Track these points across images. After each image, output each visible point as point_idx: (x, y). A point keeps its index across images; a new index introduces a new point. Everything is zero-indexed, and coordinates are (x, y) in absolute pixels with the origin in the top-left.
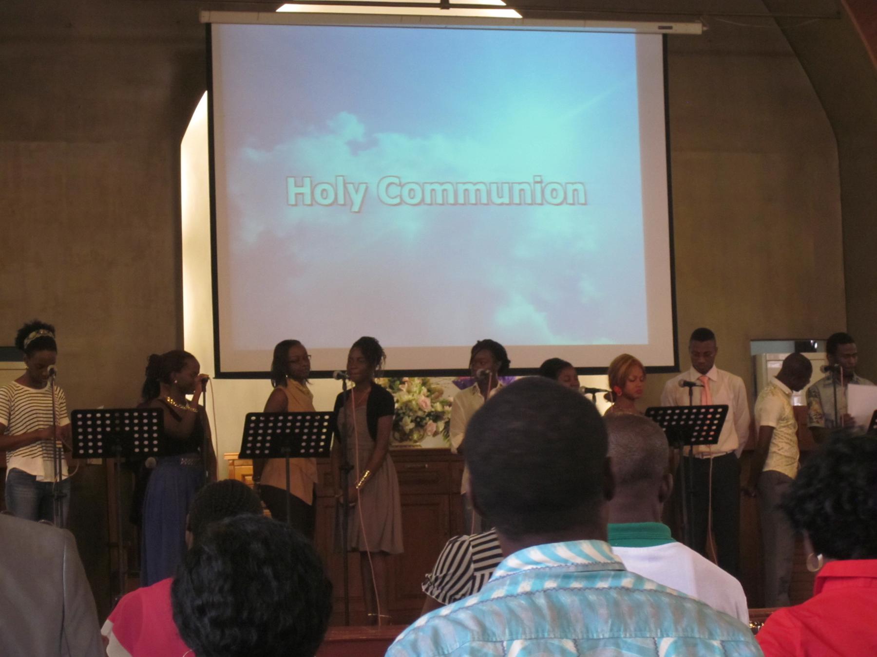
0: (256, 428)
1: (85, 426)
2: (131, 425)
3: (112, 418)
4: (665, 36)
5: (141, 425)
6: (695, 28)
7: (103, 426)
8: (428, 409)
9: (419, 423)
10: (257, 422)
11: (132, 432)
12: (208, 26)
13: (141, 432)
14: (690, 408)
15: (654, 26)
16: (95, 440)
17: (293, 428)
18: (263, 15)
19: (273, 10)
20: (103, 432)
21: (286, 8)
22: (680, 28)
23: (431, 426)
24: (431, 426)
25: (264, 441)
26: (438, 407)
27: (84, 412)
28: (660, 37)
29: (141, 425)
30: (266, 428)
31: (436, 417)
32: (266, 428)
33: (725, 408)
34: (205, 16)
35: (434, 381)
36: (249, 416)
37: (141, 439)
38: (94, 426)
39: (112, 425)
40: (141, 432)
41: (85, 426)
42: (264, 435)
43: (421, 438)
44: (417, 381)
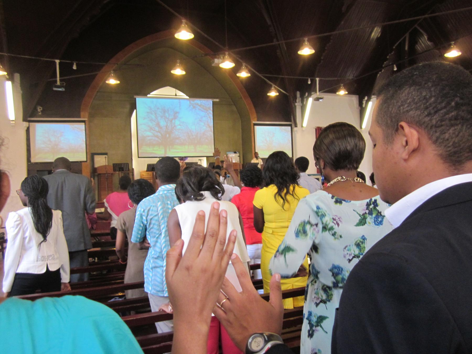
6: (217, 100)
12: (135, 99)
21: (149, 96)
22: (215, 100)
34: (135, 97)
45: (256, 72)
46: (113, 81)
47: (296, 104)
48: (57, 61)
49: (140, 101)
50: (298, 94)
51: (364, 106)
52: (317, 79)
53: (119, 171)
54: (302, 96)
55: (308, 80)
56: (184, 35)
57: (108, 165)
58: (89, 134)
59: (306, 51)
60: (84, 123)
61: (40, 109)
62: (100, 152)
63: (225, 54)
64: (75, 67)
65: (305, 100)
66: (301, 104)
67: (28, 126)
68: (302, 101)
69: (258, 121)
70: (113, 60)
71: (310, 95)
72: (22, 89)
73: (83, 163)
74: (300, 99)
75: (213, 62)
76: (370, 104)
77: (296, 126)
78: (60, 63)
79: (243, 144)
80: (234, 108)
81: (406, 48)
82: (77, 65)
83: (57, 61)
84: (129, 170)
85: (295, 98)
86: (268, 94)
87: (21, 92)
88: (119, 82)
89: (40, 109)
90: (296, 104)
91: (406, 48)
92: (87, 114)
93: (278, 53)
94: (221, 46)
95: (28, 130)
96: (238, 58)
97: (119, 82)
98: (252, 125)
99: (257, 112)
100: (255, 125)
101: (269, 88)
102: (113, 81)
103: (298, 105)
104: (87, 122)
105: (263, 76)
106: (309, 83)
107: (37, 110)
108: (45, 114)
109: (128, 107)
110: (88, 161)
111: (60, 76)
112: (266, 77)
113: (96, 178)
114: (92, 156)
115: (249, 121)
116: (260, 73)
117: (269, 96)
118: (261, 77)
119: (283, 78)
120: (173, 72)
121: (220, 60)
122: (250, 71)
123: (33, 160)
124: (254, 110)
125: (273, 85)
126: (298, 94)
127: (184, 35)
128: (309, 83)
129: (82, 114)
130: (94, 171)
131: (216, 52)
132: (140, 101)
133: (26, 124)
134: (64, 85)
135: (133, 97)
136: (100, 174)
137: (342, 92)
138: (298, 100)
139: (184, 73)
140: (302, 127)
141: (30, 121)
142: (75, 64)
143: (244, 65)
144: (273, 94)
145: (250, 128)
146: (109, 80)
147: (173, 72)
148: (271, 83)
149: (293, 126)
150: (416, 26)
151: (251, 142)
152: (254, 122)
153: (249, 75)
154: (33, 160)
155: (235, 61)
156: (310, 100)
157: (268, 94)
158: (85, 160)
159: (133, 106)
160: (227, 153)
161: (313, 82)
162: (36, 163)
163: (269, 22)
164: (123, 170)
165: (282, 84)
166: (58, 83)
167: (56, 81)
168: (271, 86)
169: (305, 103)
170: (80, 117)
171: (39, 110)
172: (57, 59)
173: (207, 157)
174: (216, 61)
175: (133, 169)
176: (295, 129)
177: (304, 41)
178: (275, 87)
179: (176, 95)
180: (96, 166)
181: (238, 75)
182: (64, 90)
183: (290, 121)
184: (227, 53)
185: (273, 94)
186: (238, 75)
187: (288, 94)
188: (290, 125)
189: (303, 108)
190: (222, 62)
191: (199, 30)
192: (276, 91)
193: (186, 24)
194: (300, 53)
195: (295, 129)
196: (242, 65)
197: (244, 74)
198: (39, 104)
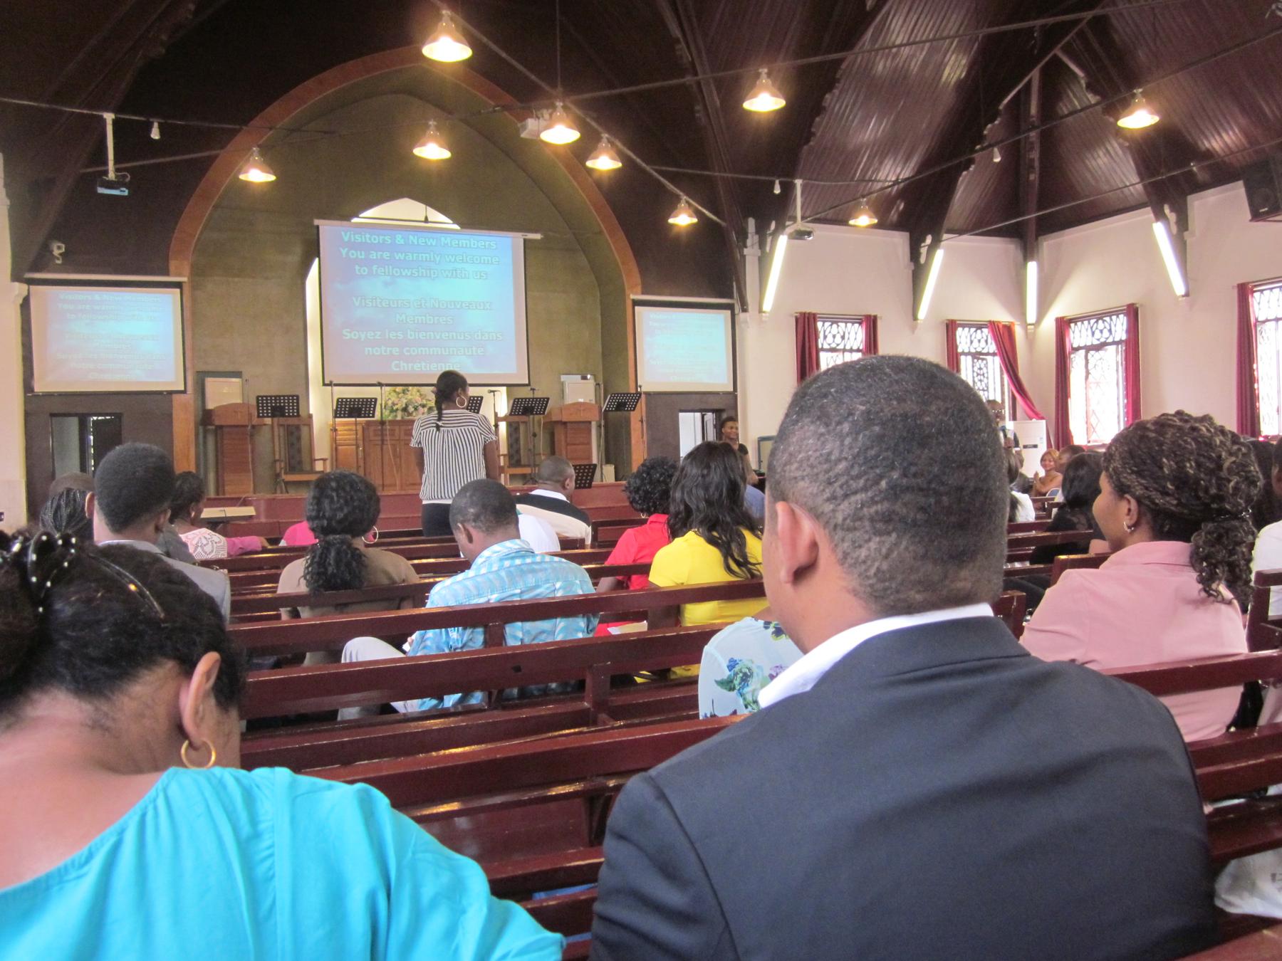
6: (538, 236)
9: (416, 409)
21: (355, 220)
22: (531, 236)
31: (424, 406)
34: (316, 222)
44: (416, 388)
45: (638, 160)
46: (257, 176)
47: (746, 251)
48: (109, 117)
49: (328, 230)
50: (751, 223)
51: (922, 260)
52: (798, 183)
53: (273, 416)
54: (761, 230)
55: (773, 184)
56: (447, 49)
58: (192, 321)
61: (58, 249)
62: (221, 369)
64: (155, 134)
65: (769, 239)
67: (25, 293)
68: (762, 244)
70: (257, 122)
71: (781, 228)
72: (8, 195)
73: (175, 397)
74: (756, 238)
75: (524, 128)
76: (939, 255)
77: (744, 310)
79: (604, 355)
80: (583, 260)
81: (1034, 110)
82: (161, 127)
83: (109, 117)
84: (298, 415)
85: (743, 235)
86: (671, 221)
87: (8, 202)
88: (272, 178)
89: (58, 249)
91: (1034, 110)
92: (187, 269)
94: (547, 88)
95: (25, 305)
97: (272, 178)
98: (629, 304)
99: (643, 271)
100: (636, 303)
101: (671, 205)
102: (257, 176)
103: (751, 252)
104: (186, 288)
105: (656, 171)
106: (777, 191)
108: (70, 261)
109: (298, 250)
110: (190, 390)
111: (116, 161)
115: (622, 293)
117: (672, 225)
118: (651, 176)
120: (418, 151)
121: (542, 123)
122: (621, 156)
123: (39, 387)
125: (684, 198)
126: (751, 223)
127: (447, 49)
128: (777, 191)
129: (173, 264)
130: (206, 418)
132: (328, 230)
133: (20, 289)
134: (128, 179)
136: (221, 427)
137: (864, 220)
138: (752, 239)
139: (445, 154)
140: (760, 311)
141: (31, 282)
142: (156, 125)
144: (683, 220)
145: (625, 311)
146: (246, 172)
147: (418, 151)
148: (678, 192)
149: (737, 308)
150: (1057, 51)
152: (632, 297)
153: (620, 165)
154: (39, 387)
156: (783, 241)
157: (671, 221)
159: (312, 249)
161: (788, 188)
163: (677, 33)
164: (283, 415)
165: (706, 194)
166: (112, 175)
167: (106, 173)
168: (678, 199)
169: (768, 249)
170: (167, 273)
171: (56, 252)
172: (107, 110)
174: (531, 123)
175: (310, 416)
176: (741, 317)
177: (758, 76)
179: (426, 221)
181: (589, 164)
182: (126, 193)
183: (731, 297)
184: (559, 104)
185: (683, 220)
186: (589, 164)
187: (723, 224)
188: (730, 307)
190: (548, 127)
191: (485, 40)
193: (452, 19)
194: (747, 105)
196: (599, 139)
197: (605, 163)
198: (57, 233)
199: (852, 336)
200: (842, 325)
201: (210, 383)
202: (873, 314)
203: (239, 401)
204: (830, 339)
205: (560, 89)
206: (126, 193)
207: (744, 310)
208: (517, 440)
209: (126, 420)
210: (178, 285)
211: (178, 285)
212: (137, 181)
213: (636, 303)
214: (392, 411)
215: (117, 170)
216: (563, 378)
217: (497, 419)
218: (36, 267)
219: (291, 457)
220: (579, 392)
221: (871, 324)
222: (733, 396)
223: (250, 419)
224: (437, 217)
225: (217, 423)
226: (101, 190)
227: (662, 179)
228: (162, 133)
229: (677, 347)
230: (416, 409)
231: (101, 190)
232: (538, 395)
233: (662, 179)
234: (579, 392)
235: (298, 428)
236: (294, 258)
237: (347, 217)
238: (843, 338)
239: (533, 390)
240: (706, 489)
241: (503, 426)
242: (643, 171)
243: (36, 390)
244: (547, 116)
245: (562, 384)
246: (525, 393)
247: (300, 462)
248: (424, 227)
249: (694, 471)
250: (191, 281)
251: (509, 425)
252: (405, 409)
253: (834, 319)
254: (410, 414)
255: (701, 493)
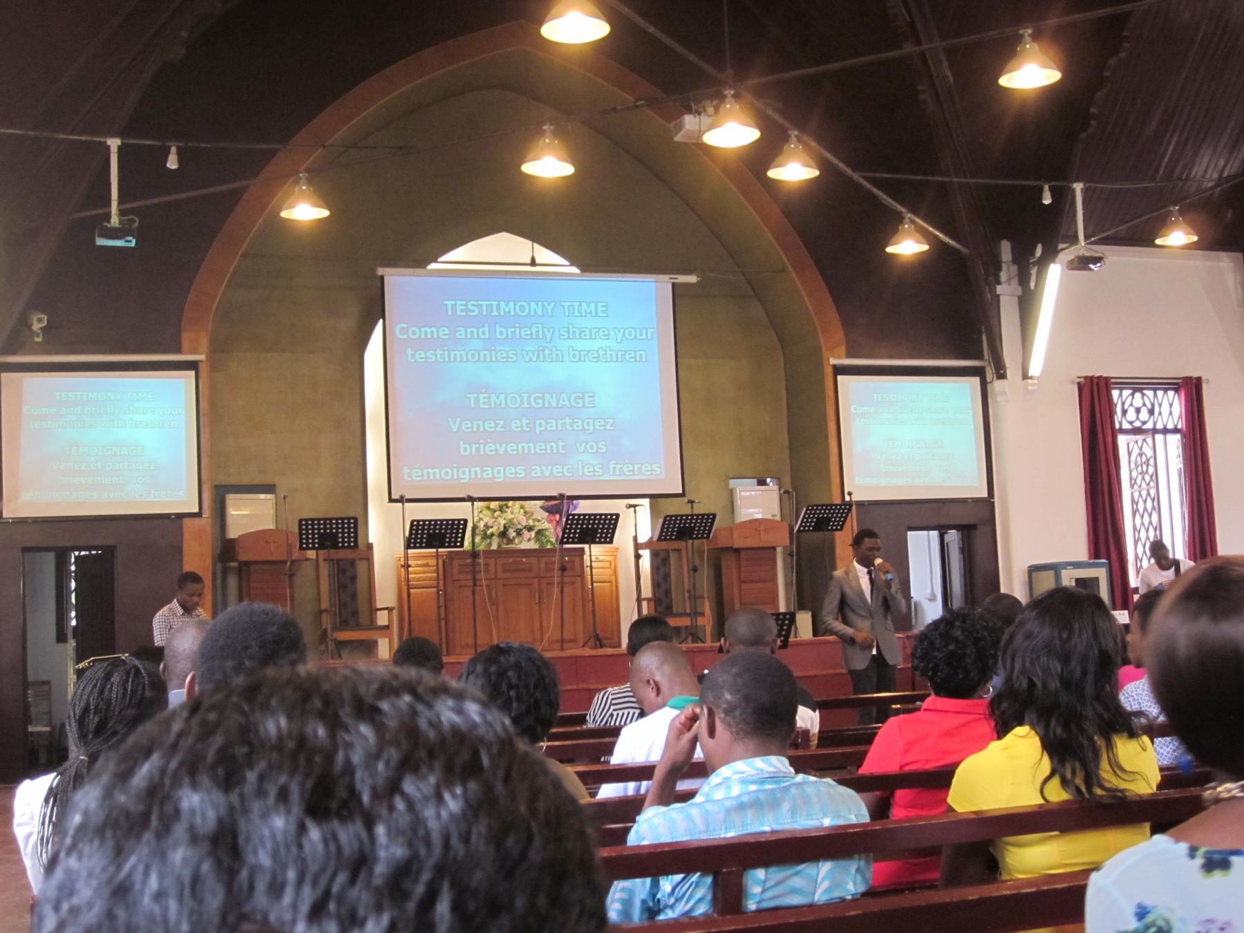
0: (417, 530)
1: (307, 529)
2: (337, 528)
3: (325, 524)
4: (673, 284)
5: (343, 528)
6: (692, 279)
7: (319, 529)
8: (524, 523)
9: (519, 533)
10: (418, 525)
11: (337, 532)
12: (382, 277)
13: (343, 533)
14: (692, 515)
15: (666, 277)
16: (313, 538)
17: (440, 529)
18: (418, 271)
19: (425, 267)
20: (319, 533)
21: (433, 266)
23: (526, 534)
24: (526, 534)
25: (422, 538)
26: (531, 523)
27: (306, 520)
28: (670, 286)
29: (343, 528)
30: (423, 529)
31: (530, 529)
32: (423, 529)
33: (714, 516)
34: (381, 271)
35: (528, 503)
36: (412, 522)
37: (343, 538)
38: (313, 529)
39: (325, 529)
40: (343, 533)
41: (307, 529)
42: (422, 534)
43: (520, 542)
45: (842, 166)
46: (304, 211)
47: (999, 289)
48: (114, 143)
49: (399, 284)
50: (1006, 250)
52: (1078, 187)
53: (322, 547)
55: (1041, 190)
57: (277, 530)
58: (211, 419)
59: (1031, 74)
60: (193, 373)
63: (722, 98)
64: (172, 163)
65: (1034, 271)
66: (1019, 291)
68: (1023, 279)
69: (849, 356)
71: (1051, 254)
73: (187, 521)
74: (1014, 269)
75: (680, 127)
77: (1001, 376)
78: (120, 149)
79: (793, 449)
82: (179, 153)
83: (114, 143)
84: (356, 546)
86: (889, 250)
88: (325, 213)
89: (38, 322)
90: (999, 289)
92: (204, 342)
93: (922, 97)
94: (710, 69)
96: (770, 112)
97: (325, 213)
98: (829, 371)
99: (847, 323)
100: (840, 370)
101: (889, 226)
102: (304, 211)
103: (1007, 292)
104: (204, 370)
105: (865, 178)
106: (1047, 201)
107: (30, 327)
108: (56, 338)
110: (206, 514)
111: (121, 200)
112: (874, 182)
113: (233, 582)
114: (218, 495)
115: (816, 358)
116: (853, 170)
117: (893, 255)
118: (860, 186)
119: (943, 183)
120: (528, 168)
121: (705, 119)
124: (833, 317)
126: (1006, 250)
128: (1047, 201)
129: (186, 337)
130: (227, 550)
131: (687, 88)
132: (399, 284)
134: (136, 225)
135: (374, 271)
136: (247, 564)
137: (1177, 237)
138: (1007, 272)
139: (568, 169)
140: (1025, 376)
142: (173, 150)
143: (793, 139)
144: (907, 247)
146: (291, 207)
147: (528, 168)
149: (990, 373)
151: (826, 438)
152: (833, 361)
153: (817, 173)
155: (763, 123)
156: (1055, 273)
157: (889, 250)
158: (197, 510)
160: (733, 483)
161: (1062, 197)
162: (22, 521)
164: (335, 546)
165: (939, 214)
166: (115, 221)
167: (108, 216)
168: (900, 219)
169: (1032, 285)
171: (36, 327)
172: (113, 136)
173: (651, 496)
174: (689, 121)
175: (370, 547)
176: (997, 386)
177: (1018, 39)
178: (913, 222)
179: (533, 263)
180: (233, 533)
181: (772, 174)
182: (133, 244)
183: (979, 356)
184: (730, 92)
185: (907, 247)
186: (772, 174)
187: (965, 251)
188: (979, 372)
189: (1027, 304)
190: (711, 127)
192: (918, 236)
194: (1005, 81)
195: (997, 386)
196: (785, 138)
197: (794, 171)
198: (36, 303)
199: (1165, 409)
200: (1150, 393)
201: (231, 499)
202: (1195, 375)
203: (272, 527)
204: (1131, 415)
205: (730, 71)
206: (133, 244)
207: (1001, 376)
208: (667, 577)
209: (121, 557)
210: (193, 366)
211: (193, 366)
212: (149, 228)
213: (840, 370)
214: (485, 536)
215: (122, 213)
216: (732, 483)
217: (637, 546)
218: (10, 350)
219: (342, 605)
220: (757, 503)
221: (1192, 390)
222: (987, 504)
223: (290, 552)
224: (545, 255)
225: (243, 556)
226: (101, 242)
227: (876, 191)
228: (180, 161)
229: (902, 433)
230: (519, 533)
231: (101, 242)
232: (699, 510)
233: (876, 191)
234: (757, 503)
235: (352, 563)
236: (348, 323)
237: (421, 263)
238: (1151, 412)
239: (691, 502)
240: (1065, 659)
241: (646, 554)
242: (850, 179)
243: (5, 515)
244: (711, 110)
245: (731, 493)
246: (679, 508)
247: (355, 613)
248: (531, 272)
249: (1043, 632)
250: (209, 357)
251: (655, 555)
252: (503, 534)
253: (1138, 386)
254: (510, 541)
255: (1057, 667)
